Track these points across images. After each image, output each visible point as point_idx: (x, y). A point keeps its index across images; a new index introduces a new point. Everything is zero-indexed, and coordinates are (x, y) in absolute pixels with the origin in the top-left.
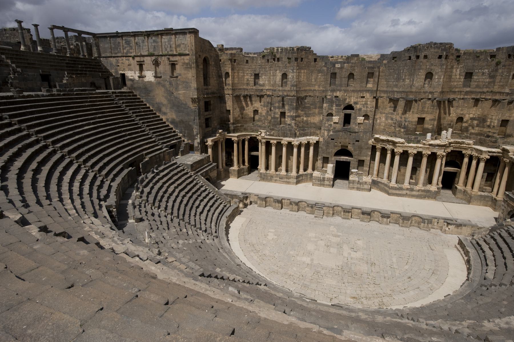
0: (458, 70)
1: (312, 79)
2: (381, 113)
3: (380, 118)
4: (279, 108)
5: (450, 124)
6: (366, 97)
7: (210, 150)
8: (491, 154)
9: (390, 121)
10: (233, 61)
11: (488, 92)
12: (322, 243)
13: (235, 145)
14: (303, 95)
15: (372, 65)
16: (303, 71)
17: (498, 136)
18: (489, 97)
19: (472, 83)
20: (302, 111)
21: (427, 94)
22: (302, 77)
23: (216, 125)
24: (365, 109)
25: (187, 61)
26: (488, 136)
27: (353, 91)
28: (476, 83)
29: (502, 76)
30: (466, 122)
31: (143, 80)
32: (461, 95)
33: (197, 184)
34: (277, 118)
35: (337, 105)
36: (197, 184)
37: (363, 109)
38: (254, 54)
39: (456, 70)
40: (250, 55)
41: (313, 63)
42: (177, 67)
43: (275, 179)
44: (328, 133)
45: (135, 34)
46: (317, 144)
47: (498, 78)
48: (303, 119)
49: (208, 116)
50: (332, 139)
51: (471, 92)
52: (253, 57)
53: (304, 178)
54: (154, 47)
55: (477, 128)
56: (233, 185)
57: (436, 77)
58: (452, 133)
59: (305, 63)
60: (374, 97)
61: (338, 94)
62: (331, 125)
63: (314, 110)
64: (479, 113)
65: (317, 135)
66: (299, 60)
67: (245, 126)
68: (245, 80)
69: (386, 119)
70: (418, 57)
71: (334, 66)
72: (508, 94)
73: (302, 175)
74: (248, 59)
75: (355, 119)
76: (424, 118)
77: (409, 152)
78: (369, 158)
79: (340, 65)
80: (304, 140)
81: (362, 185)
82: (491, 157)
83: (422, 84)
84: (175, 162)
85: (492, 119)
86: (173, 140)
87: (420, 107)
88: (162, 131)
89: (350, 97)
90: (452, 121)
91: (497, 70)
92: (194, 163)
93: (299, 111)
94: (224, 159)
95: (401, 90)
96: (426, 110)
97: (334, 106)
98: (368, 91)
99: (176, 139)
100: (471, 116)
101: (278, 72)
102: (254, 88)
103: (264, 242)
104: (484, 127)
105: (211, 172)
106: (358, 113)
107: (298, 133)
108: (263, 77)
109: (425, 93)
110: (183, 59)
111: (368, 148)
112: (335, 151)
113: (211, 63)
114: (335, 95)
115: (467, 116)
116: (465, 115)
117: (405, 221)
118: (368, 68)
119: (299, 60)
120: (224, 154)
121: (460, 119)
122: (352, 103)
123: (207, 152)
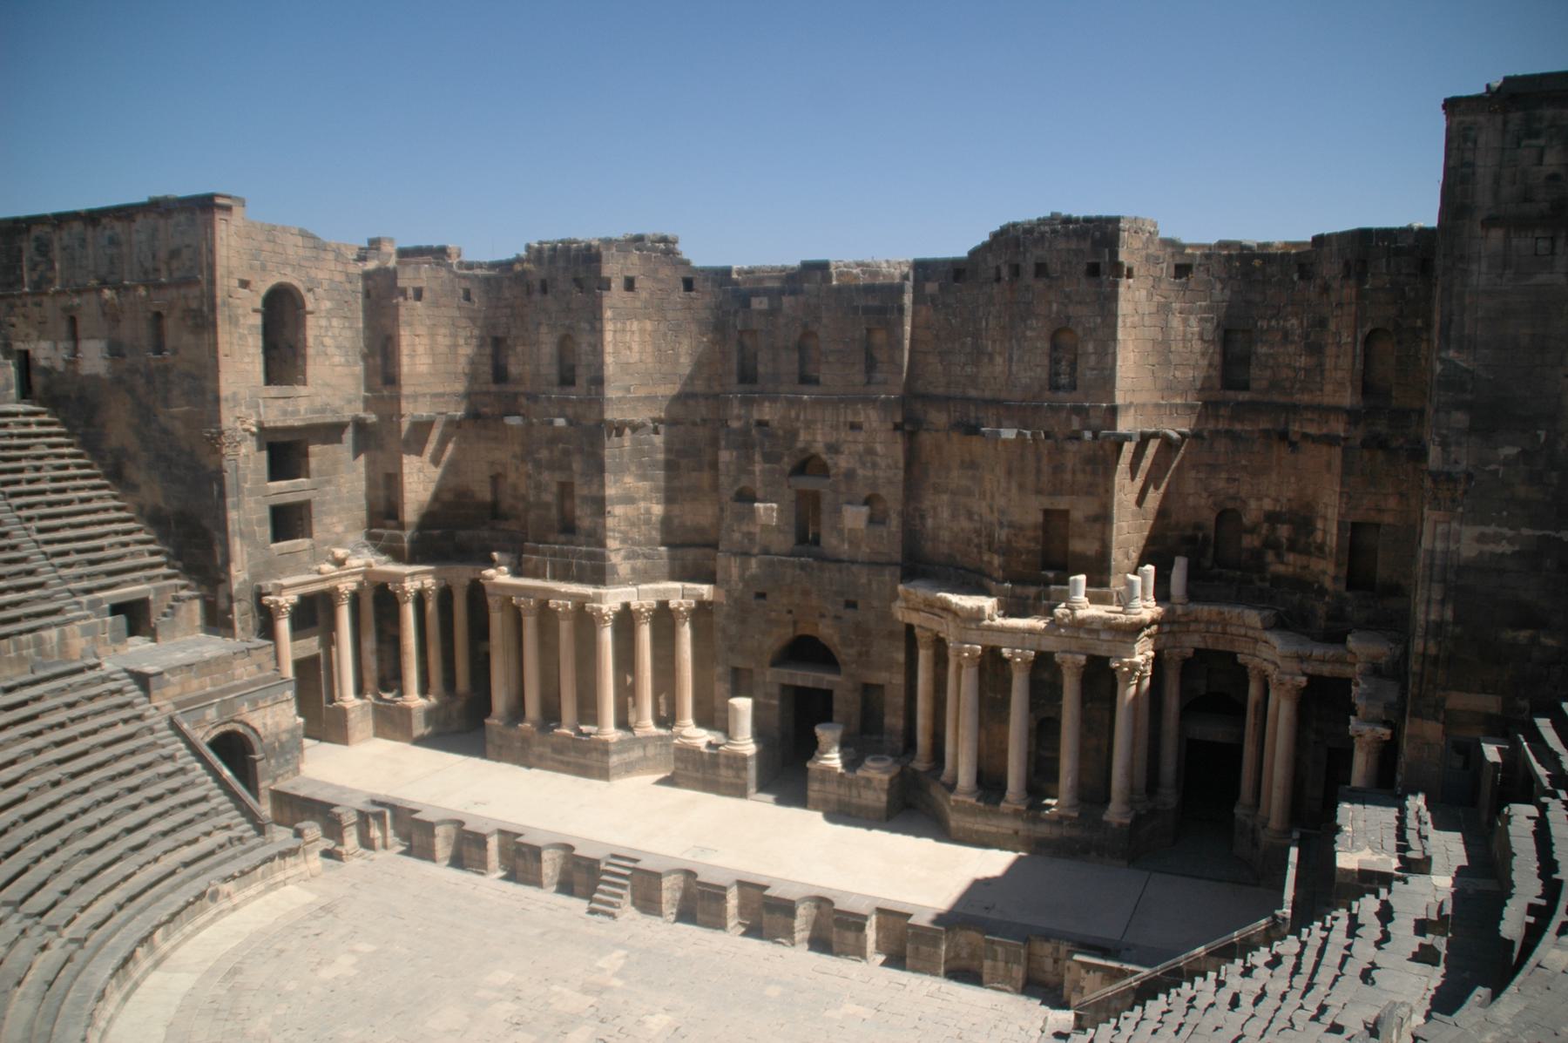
0: (1193, 321)
1: (677, 355)
2: (937, 489)
3: (935, 508)
4: (552, 466)
5: (1192, 540)
6: (866, 426)
7: (284, 626)
8: (1309, 668)
9: (965, 524)
10: (410, 293)
11: (1308, 407)
12: (505, 1009)
13: (409, 612)
14: (642, 415)
15: (874, 302)
16: (635, 325)
17: (1348, 594)
18: (1312, 430)
19: (1254, 371)
20: (643, 477)
21: (1064, 415)
22: (636, 347)
23: (339, 529)
24: (869, 473)
25: (194, 305)
26: (1322, 591)
27: (817, 403)
28: (1268, 373)
29: (1339, 345)
30: (1252, 530)
31: (75, 373)
32: (1217, 417)
33: (153, 745)
34: (547, 506)
35: (767, 458)
36: (153, 745)
37: (860, 472)
38: (493, 266)
39: (1185, 322)
40: (478, 272)
41: (679, 295)
42: (169, 324)
43: (537, 749)
44: (744, 568)
45: (61, 220)
46: (702, 611)
47: (1331, 350)
48: (648, 511)
49: (290, 498)
50: (761, 596)
51: (1254, 408)
52: (487, 280)
53: (651, 751)
54: (112, 262)
55: (1290, 557)
56: (364, 765)
57: (1090, 348)
58: (1193, 575)
59: (644, 295)
60: (897, 427)
61: (767, 412)
62: (750, 536)
63: (694, 474)
64: (1290, 495)
65: (709, 578)
66: (617, 285)
67: (463, 534)
68: (463, 360)
69: (954, 516)
70: (1016, 270)
71: (746, 304)
72: (1353, 416)
73: (645, 742)
74: (467, 284)
75: (837, 511)
76: (1066, 513)
77: (1006, 652)
78: (899, 679)
79: (765, 300)
80: (641, 596)
81: (854, 792)
82: (1312, 679)
83: (1042, 373)
84: (95, 661)
85: (1325, 518)
86: (136, 581)
87: (1046, 467)
88: (101, 549)
89: (809, 425)
90: (1198, 527)
91: (1322, 323)
92: (173, 670)
93: (629, 480)
94: (371, 662)
95: (988, 394)
96: (1068, 477)
97: (757, 457)
98: (868, 401)
99: (149, 579)
100: (1268, 505)
101: (544, 329)
102: (493, 388)
103: (292, 986)
104: (1306, 551)
105: (255, 707)
106: (843, 488)
107: (624, 568)
108: (519, 349)
109: (1055, 409)
110: (186, 298)
111: (891, 635)
112: (774, 640)
113: (309, 306)
114: (756, 416)
115: (1253, 504)
116: (1244, 502)
117: (924, 949)
118: (867, 310)
119: (617, 285)
120: (369, 644)
121: (1227, 516)
122: (819, 447)
123: (267, 630)
